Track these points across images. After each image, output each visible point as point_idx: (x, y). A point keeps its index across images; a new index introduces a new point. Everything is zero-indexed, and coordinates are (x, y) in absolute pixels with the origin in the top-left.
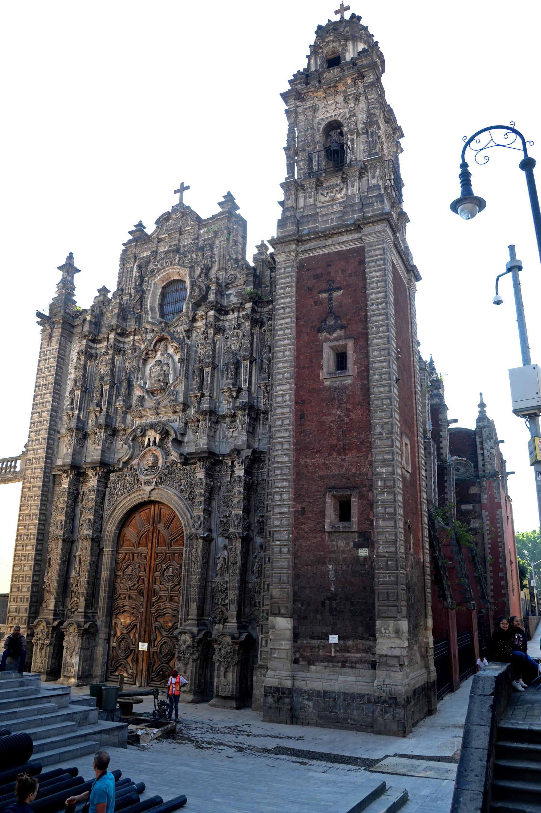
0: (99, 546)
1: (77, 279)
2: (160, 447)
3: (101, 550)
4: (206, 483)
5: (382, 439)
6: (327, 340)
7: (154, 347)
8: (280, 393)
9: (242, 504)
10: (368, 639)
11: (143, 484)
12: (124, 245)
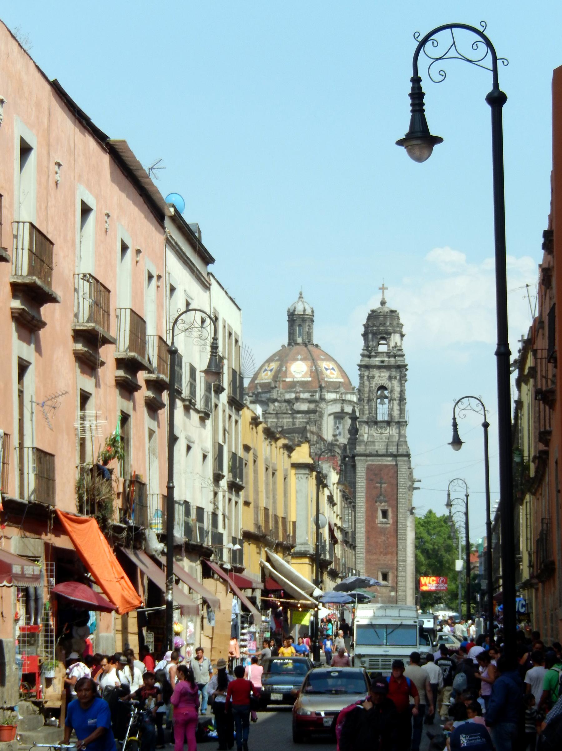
6: (379, 506)
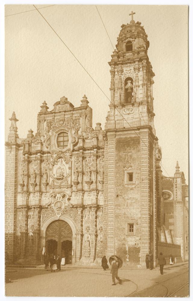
11: (56, 214)
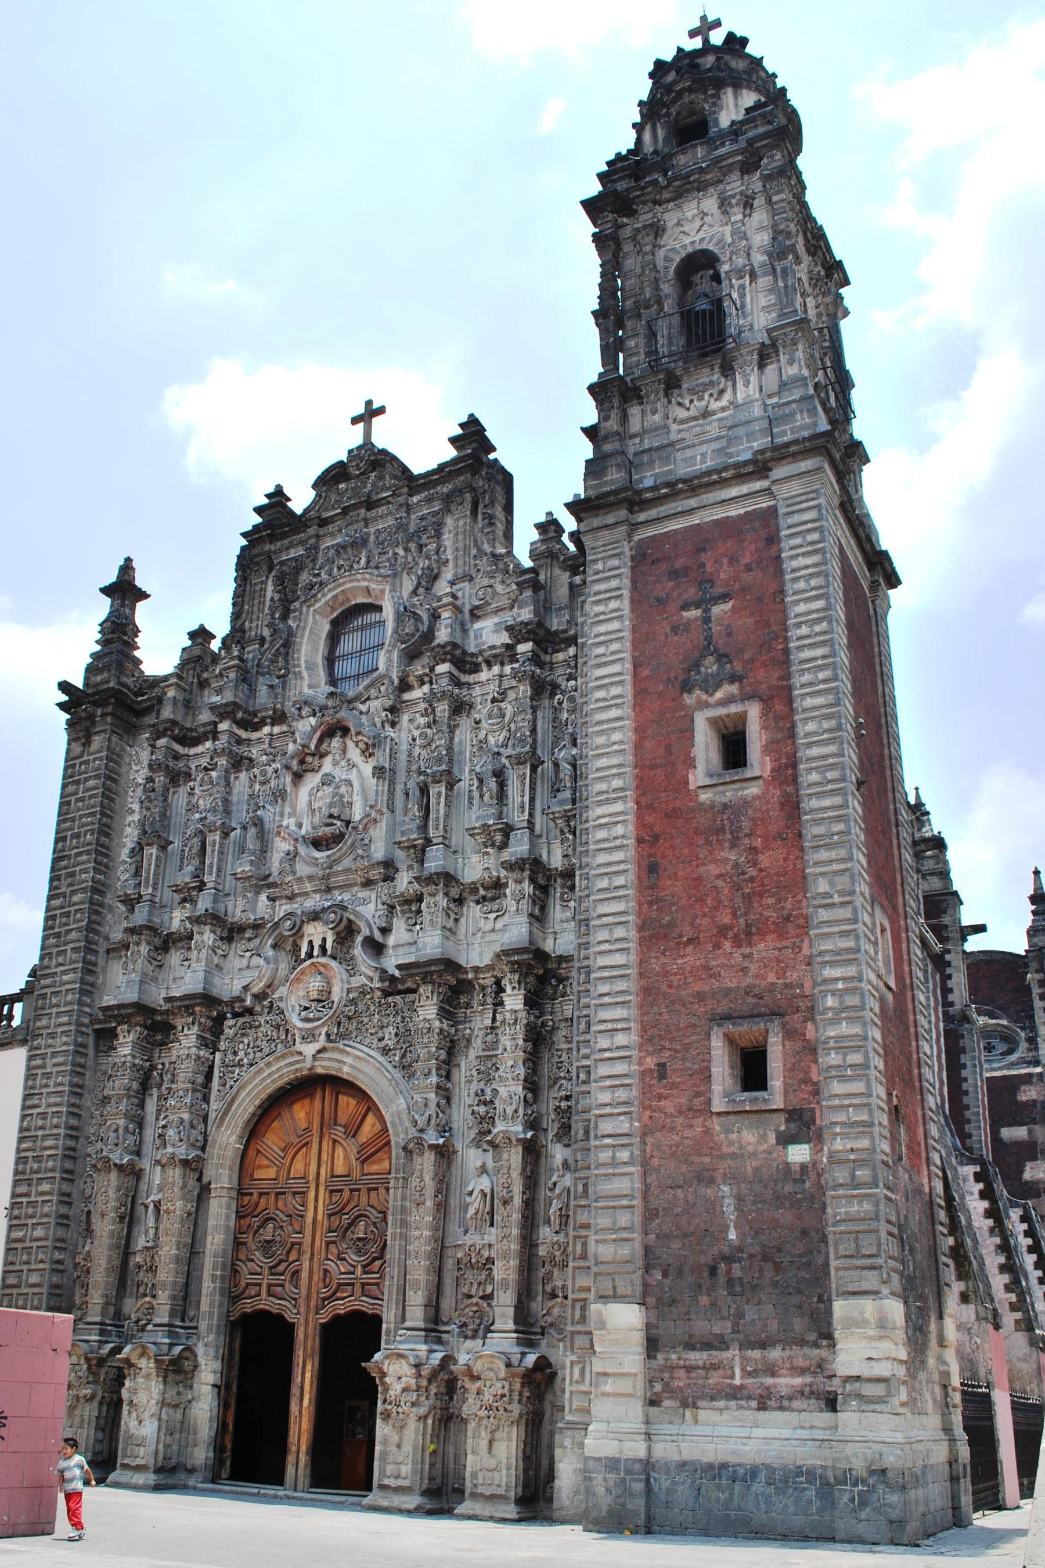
0: (199, 1179)
1: (142, 613)
2: (334, 958)
3: (205, 1190)
4: (441, 1030)
5: (832, 905)
6: (703, 705)
7: (317, 747)
8: (603, 821)
9: (521, 1071)
10: (816, 1345)
11: (298, 1040)
12: (245, 535)
